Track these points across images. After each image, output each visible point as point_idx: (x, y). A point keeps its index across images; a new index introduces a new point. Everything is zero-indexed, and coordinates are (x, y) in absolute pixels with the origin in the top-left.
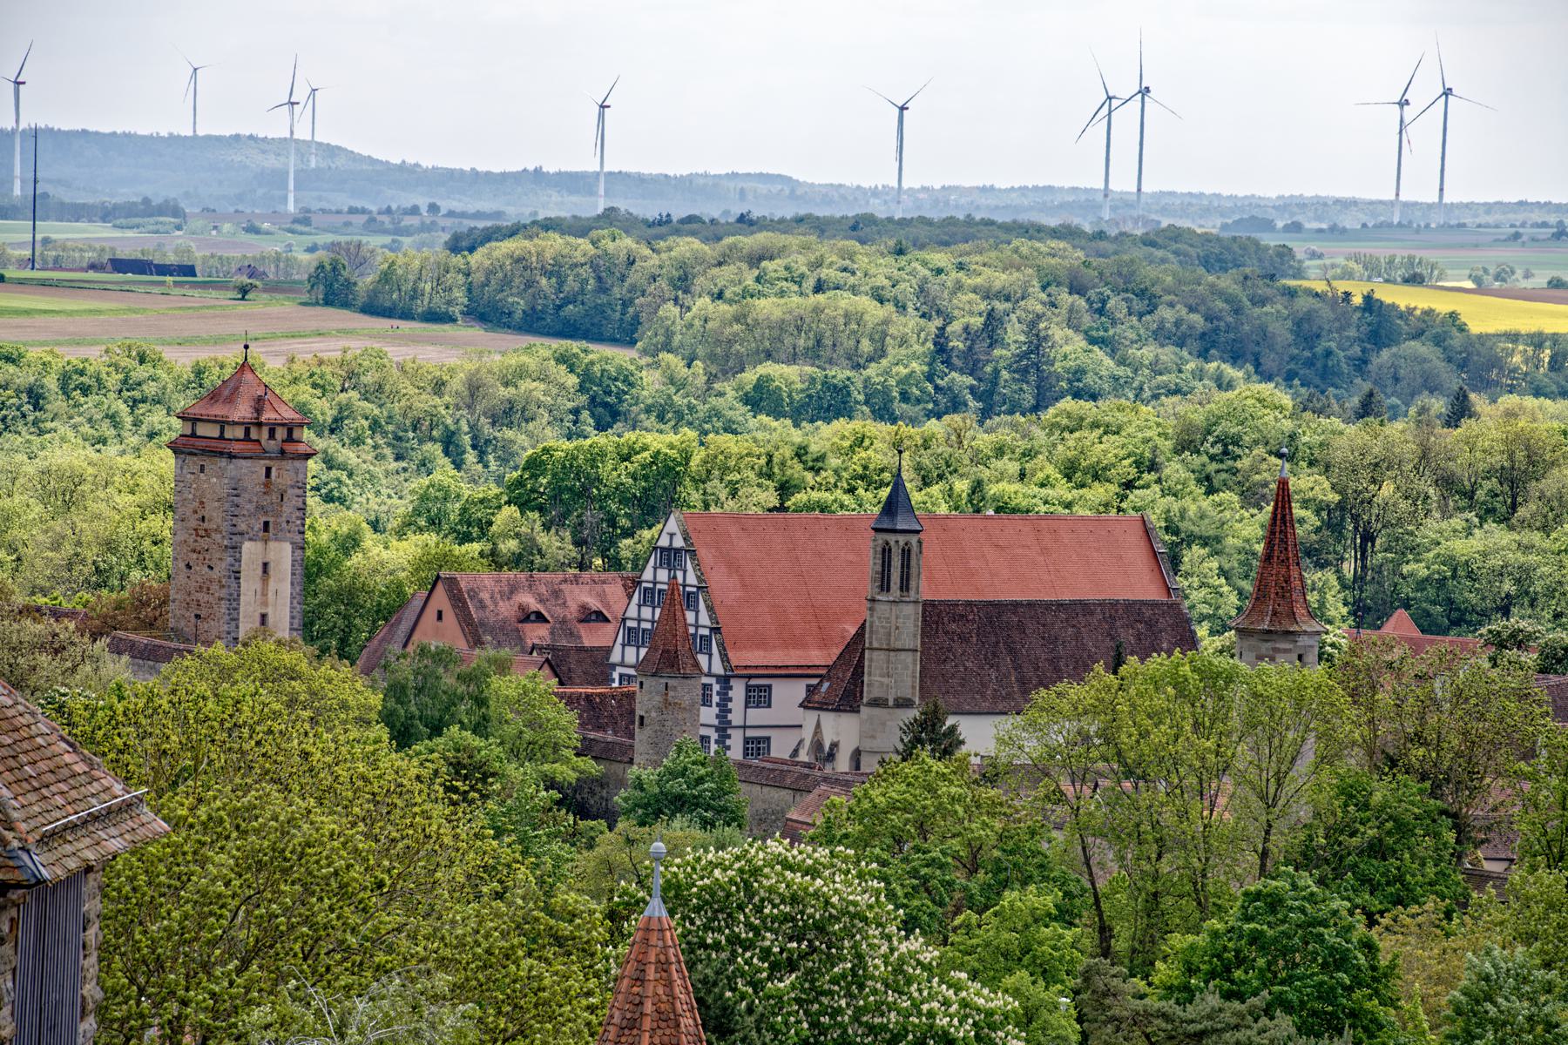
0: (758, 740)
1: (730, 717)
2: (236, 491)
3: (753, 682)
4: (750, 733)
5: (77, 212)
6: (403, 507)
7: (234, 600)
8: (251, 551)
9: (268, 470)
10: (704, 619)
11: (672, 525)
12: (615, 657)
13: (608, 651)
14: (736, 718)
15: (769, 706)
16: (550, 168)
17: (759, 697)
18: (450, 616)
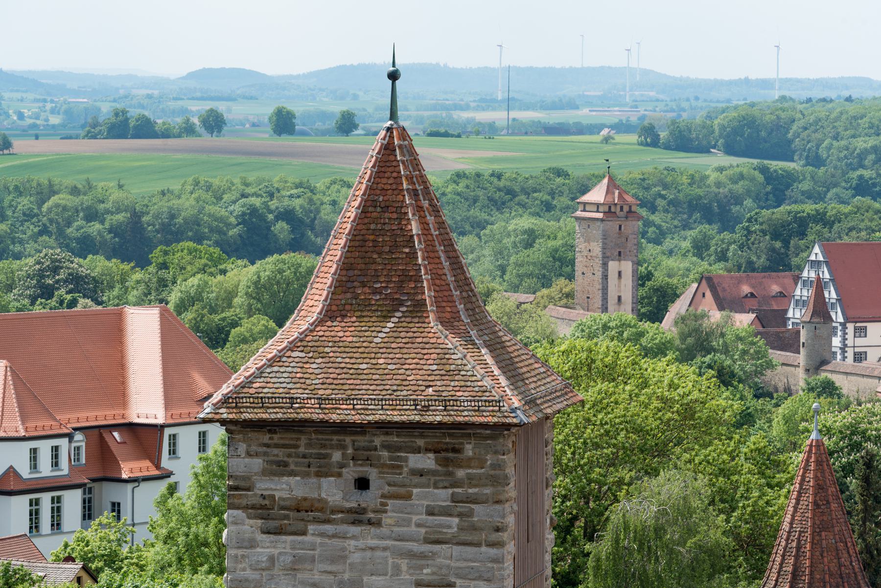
0: (861, 353)
1: (847, 342)
2: (605, 237)
3: (858, 325)
4: (857, 350)
5: (527, 107)
6: (686, 244)
7: (605, 290)
8: (613, 266)
9: (620, 226)
10: (834, 295)
11: (817, 249)
12: (790, 314)
13: (786, 311)
14: (849, 342)
15: (866, 336)
16: (753, 77)
17: (861, 332)
18: (708, 294)
